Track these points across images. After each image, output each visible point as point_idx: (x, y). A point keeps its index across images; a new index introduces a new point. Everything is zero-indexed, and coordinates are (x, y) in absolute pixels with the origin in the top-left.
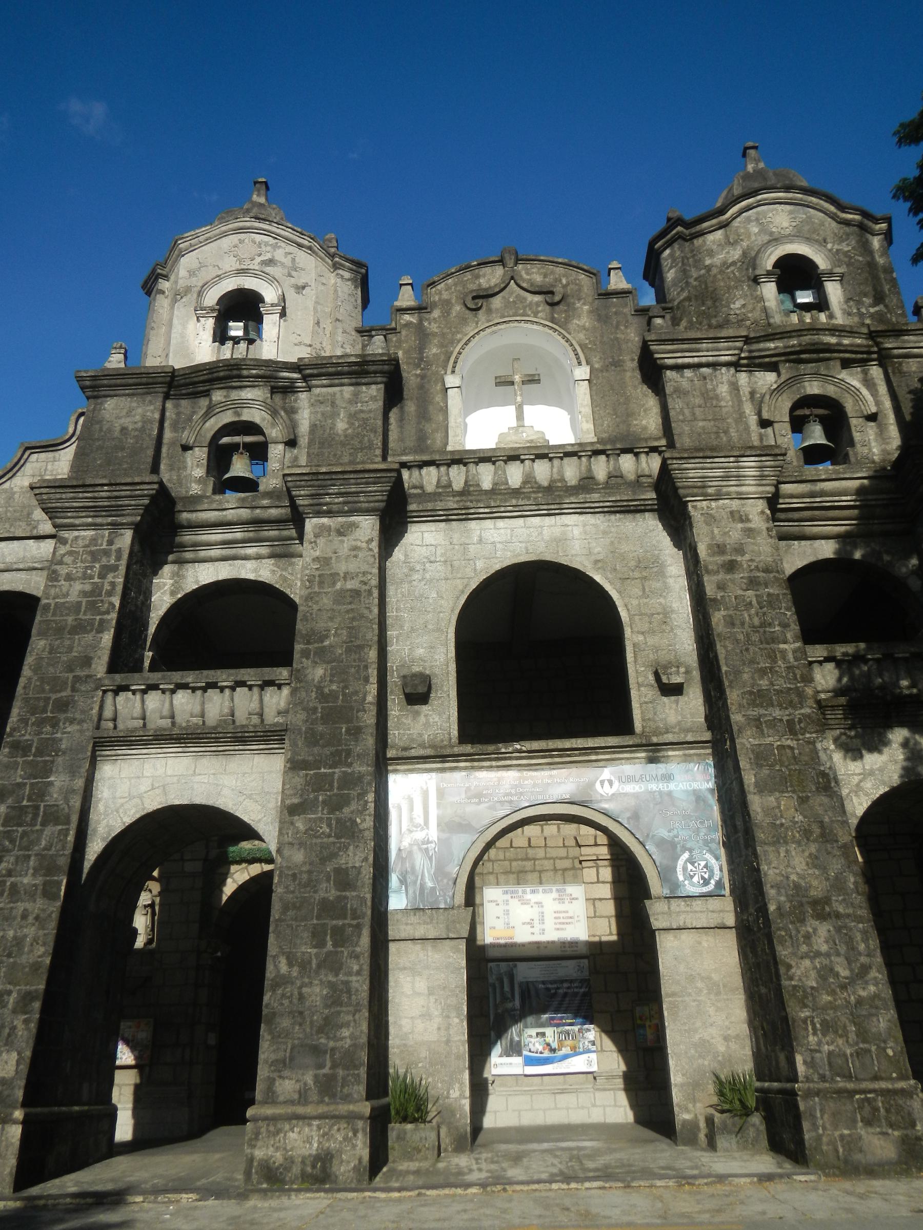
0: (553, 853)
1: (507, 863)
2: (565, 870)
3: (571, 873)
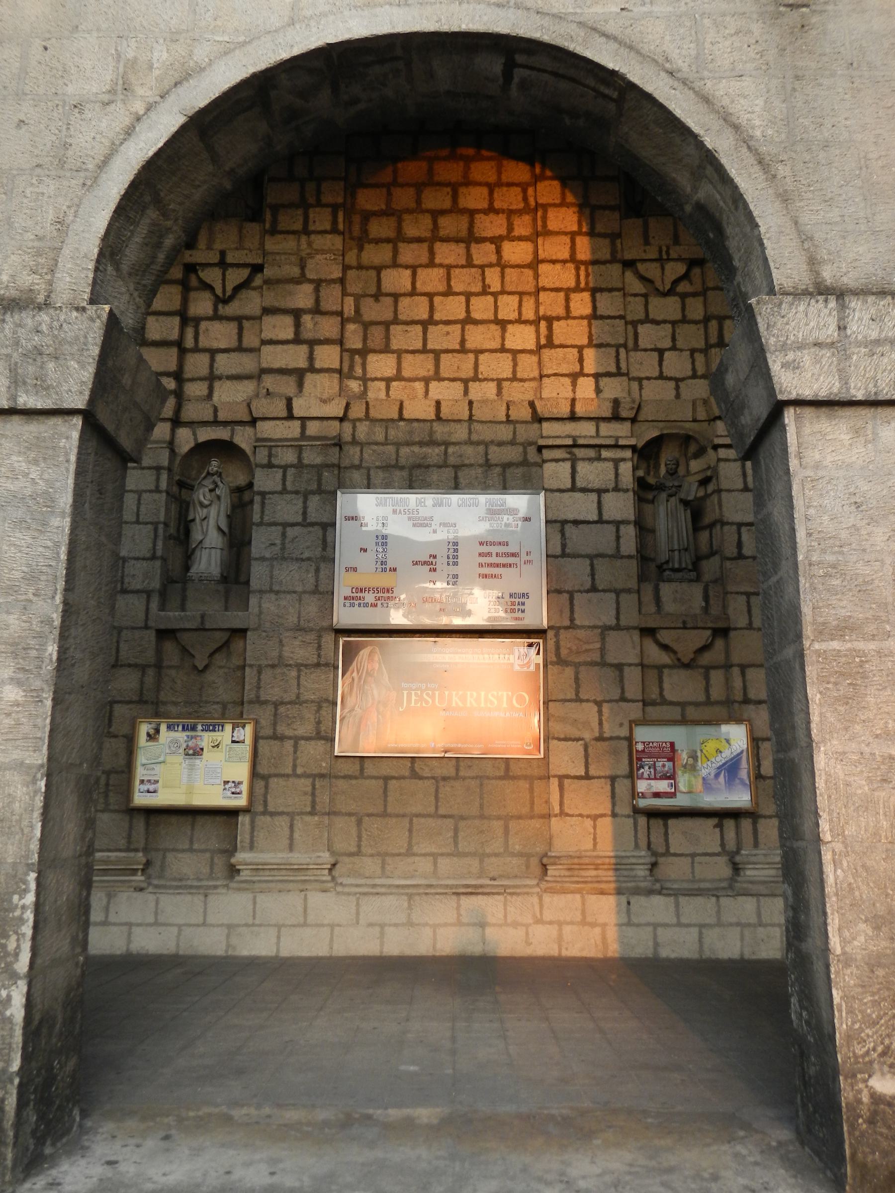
0: (485, 433)
1: (391, 449)
2: (506, 466)
3: (520, 471)
